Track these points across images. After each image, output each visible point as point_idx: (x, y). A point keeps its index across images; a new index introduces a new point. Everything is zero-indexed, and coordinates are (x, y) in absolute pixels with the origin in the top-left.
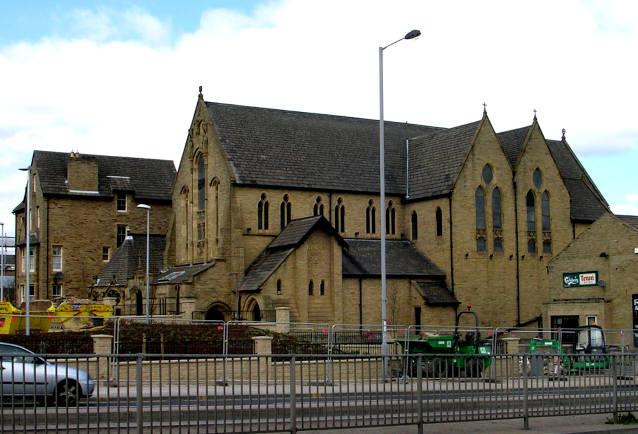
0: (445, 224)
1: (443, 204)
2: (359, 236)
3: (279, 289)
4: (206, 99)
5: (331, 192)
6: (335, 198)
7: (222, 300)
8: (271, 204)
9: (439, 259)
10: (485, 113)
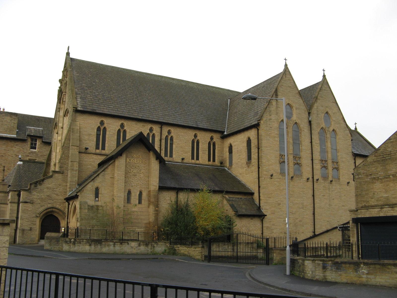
0: (254, 150)
1: (252, 134)
2: (185, 161)
3: (97, 195)
4: (71, 56)
5: (162, 124)
6: (165, 130)
7: (57, 206)
8: (108, 130)
9: (246, 176)
10: (286, 65)
